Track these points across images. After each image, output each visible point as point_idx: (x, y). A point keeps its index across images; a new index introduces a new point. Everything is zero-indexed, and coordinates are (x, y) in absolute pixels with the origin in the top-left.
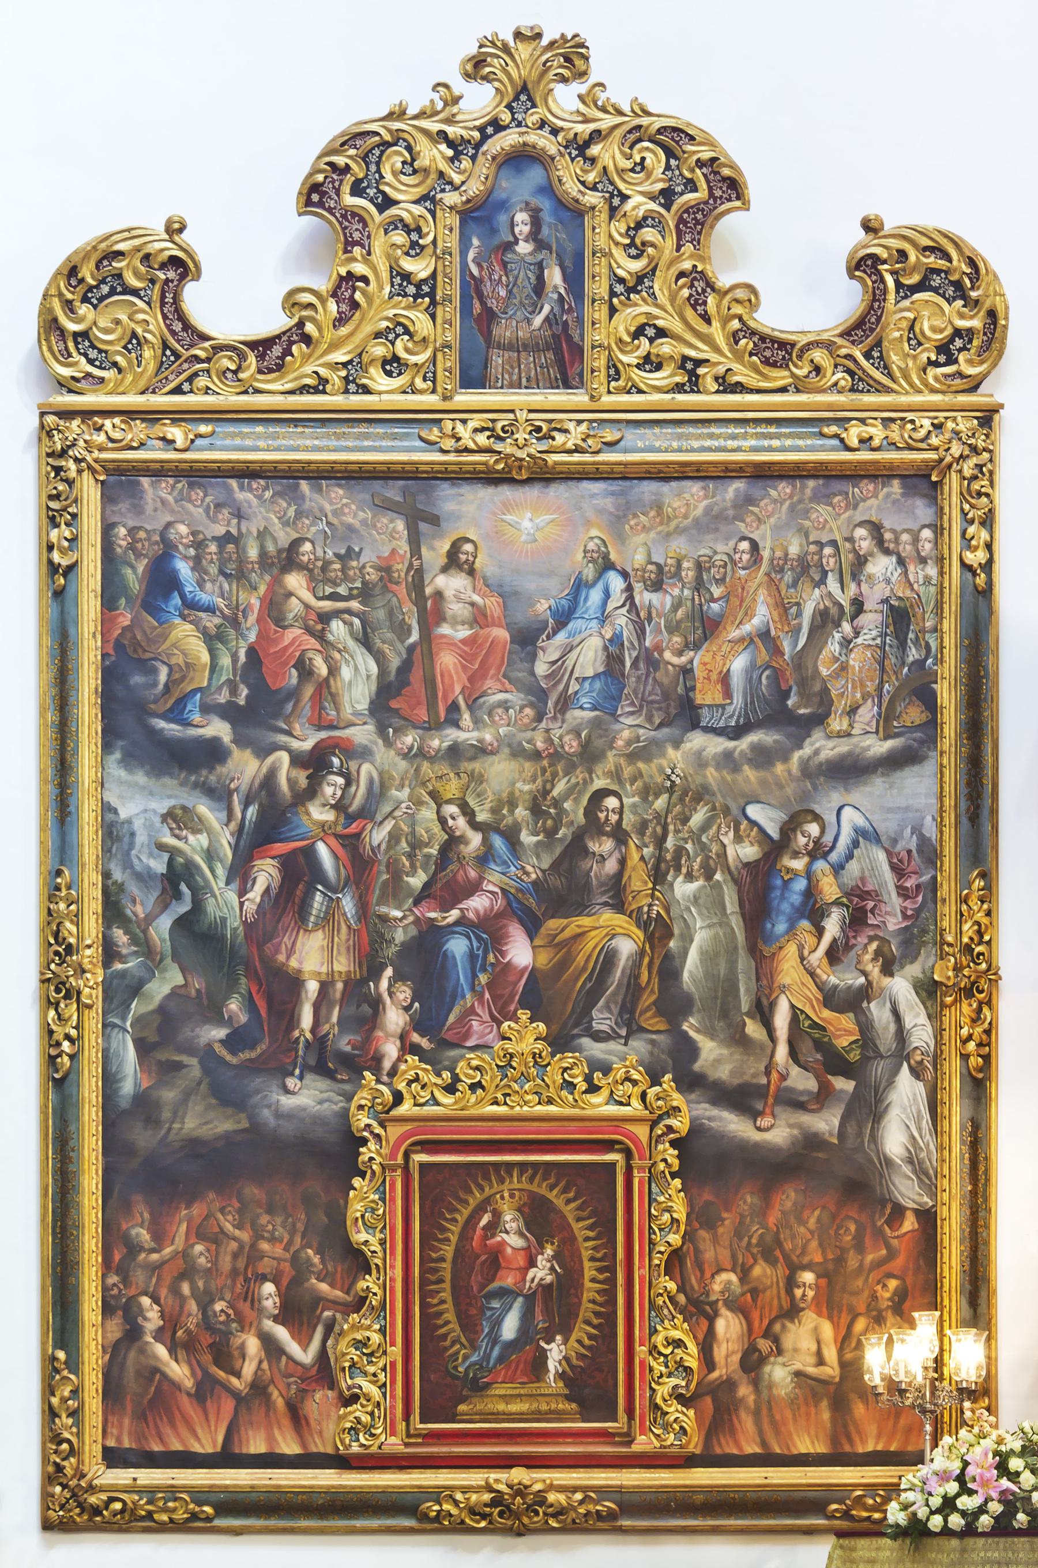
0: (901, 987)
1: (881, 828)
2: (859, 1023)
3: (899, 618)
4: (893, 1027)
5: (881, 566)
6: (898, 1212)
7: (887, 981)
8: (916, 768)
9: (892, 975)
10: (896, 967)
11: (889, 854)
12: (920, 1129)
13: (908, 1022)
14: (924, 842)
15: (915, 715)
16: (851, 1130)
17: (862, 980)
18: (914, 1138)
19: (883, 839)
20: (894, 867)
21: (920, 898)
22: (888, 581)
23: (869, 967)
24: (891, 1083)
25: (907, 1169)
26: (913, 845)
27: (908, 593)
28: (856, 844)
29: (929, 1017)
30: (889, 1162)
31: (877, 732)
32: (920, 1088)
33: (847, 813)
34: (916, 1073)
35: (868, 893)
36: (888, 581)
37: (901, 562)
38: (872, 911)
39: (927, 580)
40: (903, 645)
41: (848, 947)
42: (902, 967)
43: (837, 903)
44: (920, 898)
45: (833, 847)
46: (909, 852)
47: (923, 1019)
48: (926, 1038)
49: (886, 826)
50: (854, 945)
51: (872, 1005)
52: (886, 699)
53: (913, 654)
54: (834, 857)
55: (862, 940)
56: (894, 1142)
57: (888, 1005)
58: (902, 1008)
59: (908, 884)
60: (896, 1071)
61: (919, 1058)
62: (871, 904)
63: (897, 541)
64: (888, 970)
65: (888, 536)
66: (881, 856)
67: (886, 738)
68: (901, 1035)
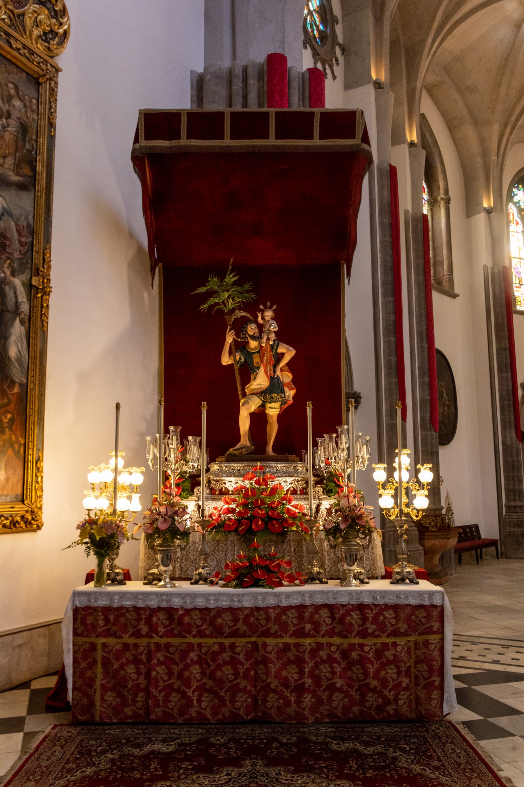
0: (17, 282)
3: (24, 129)
4: (14, 299)
5: (17, 103)
6: (13, 382)
7: (12, 279)
9: (14, 277)
10: (16, 274)
11: (16, 224)
12: (22, 347)
13: (20, 299)
14: (29, 225)
15: (27, 170)
17: (3, 275)
18: (19, 351)
20: (18, 231)
21: (26, 248)
22: (20, 111)
23: (6, 270)
24: (12, 325)
25: (16, 364)
26: (25, 224)
27: (27, 120)
29: (28, 299)
30: (10, 359)
31: (13, 171)
32: (23, 329)
34: (22, 323)
36: (20, 111)
37: (25, 106)
38: (9, 246)
40: (24, 140)
42: (18, 275)
44: (26, 248)
46: (23, 227)
47: (25, 300)
48: (26, 308)
49: (16, 212)
51: (7, 287)
53: (28, 146)
56: (13, 352)
57: (13, 290)
58: (18, 293)
59: (22, 240)
60: (14, 320)
63: (24, 97)
64: (13, 274)
65: (21, 93)
66: (13, 224)
67: (17, 175)
68: (17, 304)
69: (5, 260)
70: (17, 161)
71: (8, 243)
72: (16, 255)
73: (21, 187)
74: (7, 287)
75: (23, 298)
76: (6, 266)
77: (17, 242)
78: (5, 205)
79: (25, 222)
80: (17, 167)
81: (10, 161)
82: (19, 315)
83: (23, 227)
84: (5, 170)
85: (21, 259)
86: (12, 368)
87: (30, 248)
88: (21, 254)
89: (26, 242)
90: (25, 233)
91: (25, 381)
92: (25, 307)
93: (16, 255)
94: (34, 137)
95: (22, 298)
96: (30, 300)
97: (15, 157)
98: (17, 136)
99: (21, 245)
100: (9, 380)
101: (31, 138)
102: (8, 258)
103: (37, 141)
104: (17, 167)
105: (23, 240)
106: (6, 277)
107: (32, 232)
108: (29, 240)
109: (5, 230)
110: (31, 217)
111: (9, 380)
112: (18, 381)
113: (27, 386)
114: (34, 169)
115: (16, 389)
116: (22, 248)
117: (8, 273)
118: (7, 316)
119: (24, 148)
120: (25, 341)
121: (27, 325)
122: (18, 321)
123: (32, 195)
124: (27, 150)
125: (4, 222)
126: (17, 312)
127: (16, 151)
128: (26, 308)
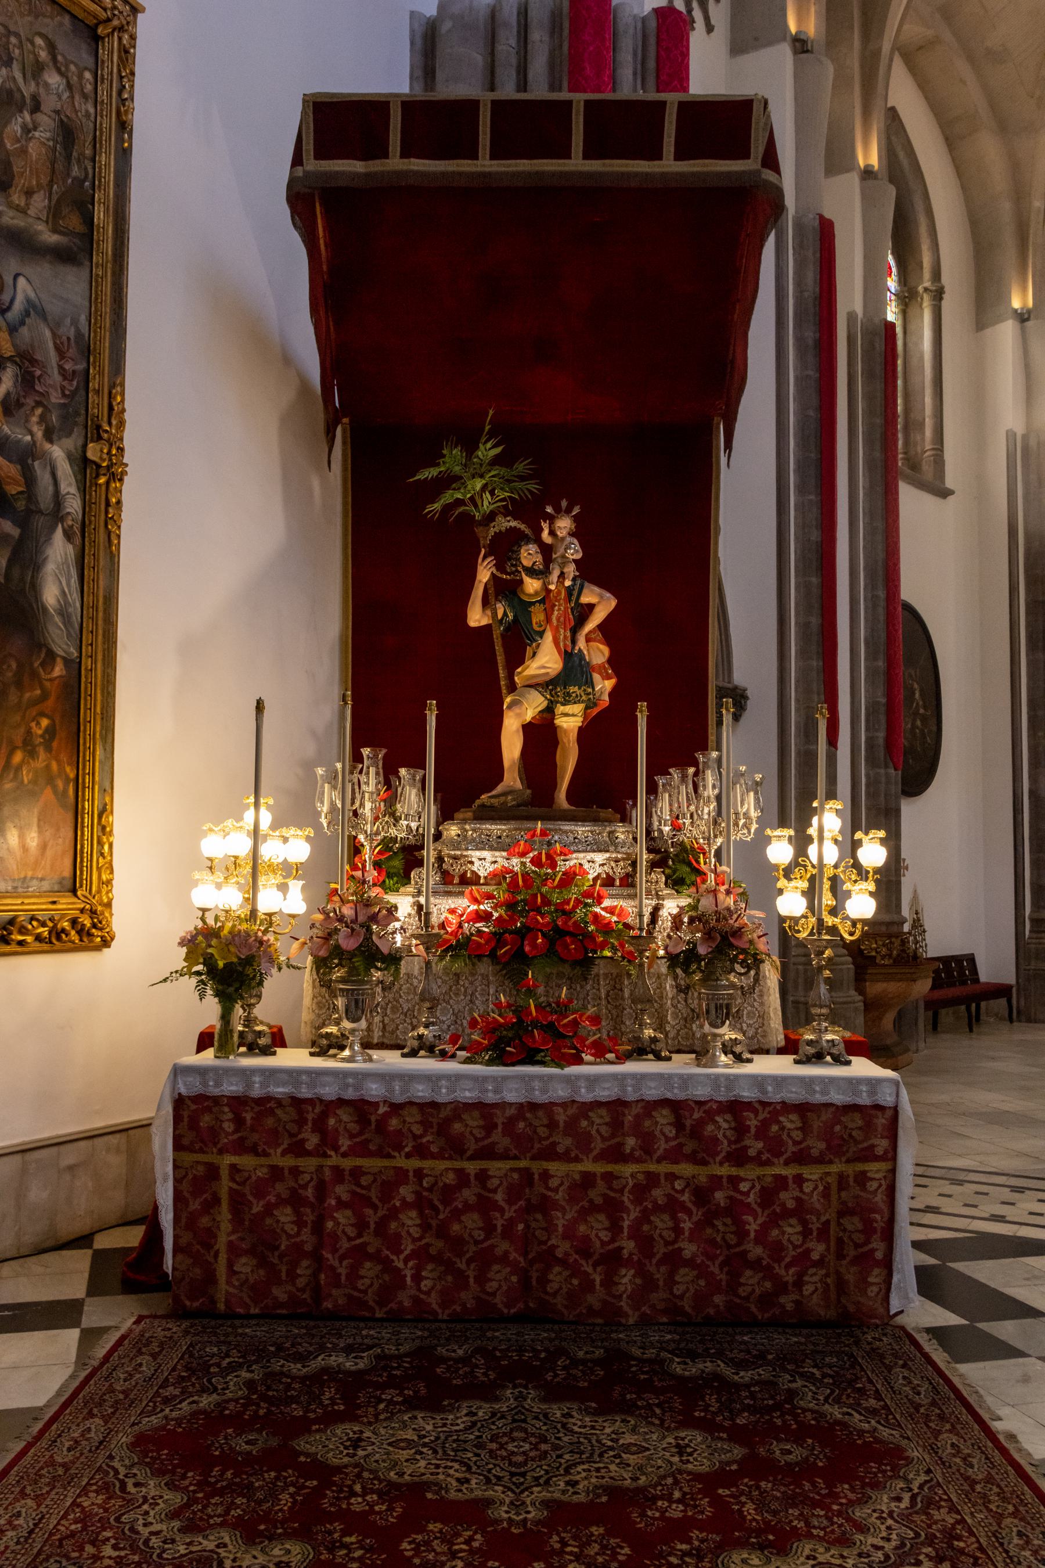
1: (48, 307)
2: (24, 475)
3: (67, 133)
4: (51, 488)
6: (51, 656)
7: (47, 446)
8: (75, 269)
10: (55, 437)
12: (69, 585)
14: (79, 335)
15: (74, 222)
16: (16, 572)
17: (28, 438)
18: (64, 592)
19: (49, 318)
20: (57, 348)
21: (75, 383)
23: (35, 429)
25: (57, 619)
27: (73, 116)
28: (27, 314)
30: (45, 610)
31: (47, 222)
32: (70, 549)
33: (21, 281)
34: (68, 536)
35: (36, 361)
38: (39, 378)
39: (87, 115)
40: (68, 157)
41: (19, 405)
42: (60, 439)
43: (10, 359)
44: (75, 383)
45: (9, 308)
46: (69, 339)
47: (73, 490)
48: (75, 506)
49: (54, 308)
50: (23, 405)
51: (36, 463)
52: (55, 197)
53: (75, 171)
54: (9, 315)
55: (30, 401)
58: (60, 474)
59: (67, 367)
60: (52, 530)
61: (70, 523)
62: (38, 373)
66: (48, 333)
67: (55, 231)
68: (58, 499)
69: (33, 409)
70: (53, 203)
71: (38, 373)
72: (56, 398)
73: (63, 256)
74: (36, 463)
75: (70, 485)
76: (35, 419)
77: (56, 371)
78: (32, 295)
79: (73, 330)
80: (54, 216)
81: (39, 202)
82: (62, 519)
83: (69, 339)
84: (30, 220)
85: (64, 406)
86: (51, 629)
87: (82, 384)
88: (64, 395)
89: (74, 372)
90: (72, 352)
91: (76, 654)
92: (73, 505)
93: (56, 398)
94: (88, 152)
95: (69, 486)
96: (83, 490)
97: (50, 194)
98: (54, 149)
99: (65, 378)
100: (44, 651)
101: (82, 154)
102: (39, 404)
103: (94, 160)
104: (54, 215)
105: (68, 366)
106: (34, 442)
107: (87, 351)
108: (81, 367)
109: (32, 346)
110: (83, 318)
111: (44, 651)
112: (62, 653)
113: (80, 663)
114: (89, 220)
115: (58, 670)
116: (65, 383)
117: (39, 435)
118: (39, 522)
119: (68, 175)
120: (74, 573)
121: (78, 540)
122: (59, 534)
123: (85, 273)
124: (75, 179)
125: (29, 329)
126: (57, 513)
127: (52, 181)
128: (75, 506)
